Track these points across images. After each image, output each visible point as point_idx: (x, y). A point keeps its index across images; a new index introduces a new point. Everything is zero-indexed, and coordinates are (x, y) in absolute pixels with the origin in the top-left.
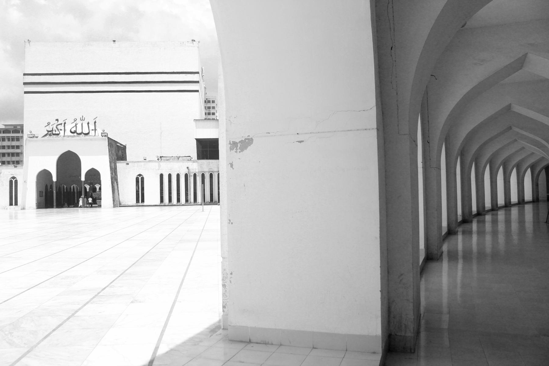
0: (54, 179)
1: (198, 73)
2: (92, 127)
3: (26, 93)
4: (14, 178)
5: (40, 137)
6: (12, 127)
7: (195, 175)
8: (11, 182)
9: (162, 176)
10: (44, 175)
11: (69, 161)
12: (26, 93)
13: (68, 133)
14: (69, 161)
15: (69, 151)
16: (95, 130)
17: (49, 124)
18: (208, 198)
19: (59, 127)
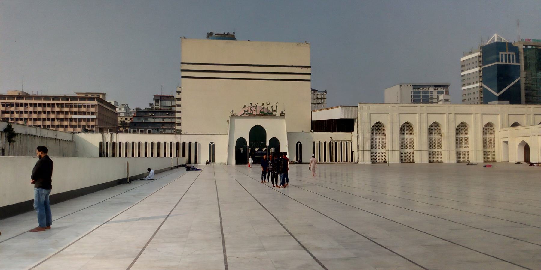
0: (248, 144)
1: (310, 67)
2: (274, 109)
3: (182, 77)
4: (212, 143)
5: (239, 115)
6: (84, 96)
7: (336, 143)
8: (210, 146)
9: (314, 143)
10: (241, 142)
11: (258, 133)
12: (182, 77)
13: (258, 113)
14: (258, 133)
15: (258, 126)
16: (276, 111)
17: (245, 106)
18: (344, 159)
19: (252, 109)
